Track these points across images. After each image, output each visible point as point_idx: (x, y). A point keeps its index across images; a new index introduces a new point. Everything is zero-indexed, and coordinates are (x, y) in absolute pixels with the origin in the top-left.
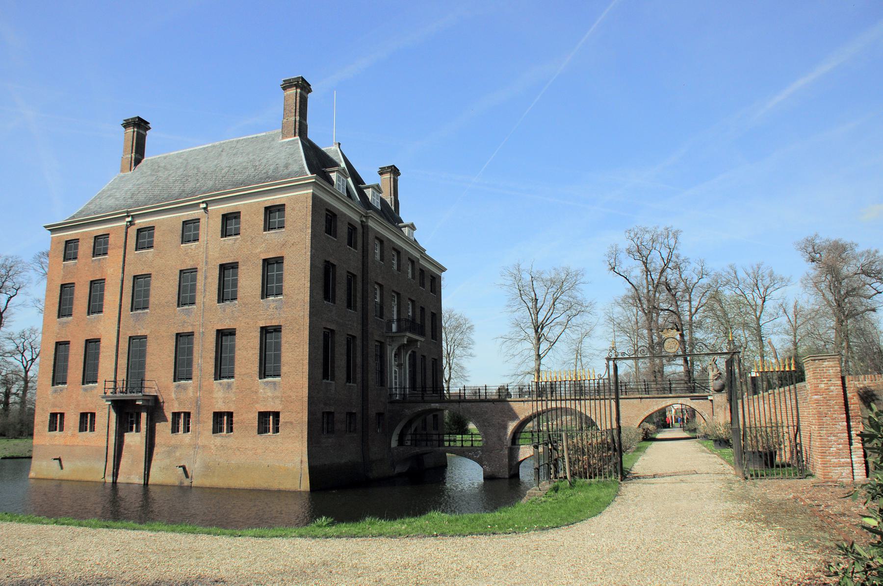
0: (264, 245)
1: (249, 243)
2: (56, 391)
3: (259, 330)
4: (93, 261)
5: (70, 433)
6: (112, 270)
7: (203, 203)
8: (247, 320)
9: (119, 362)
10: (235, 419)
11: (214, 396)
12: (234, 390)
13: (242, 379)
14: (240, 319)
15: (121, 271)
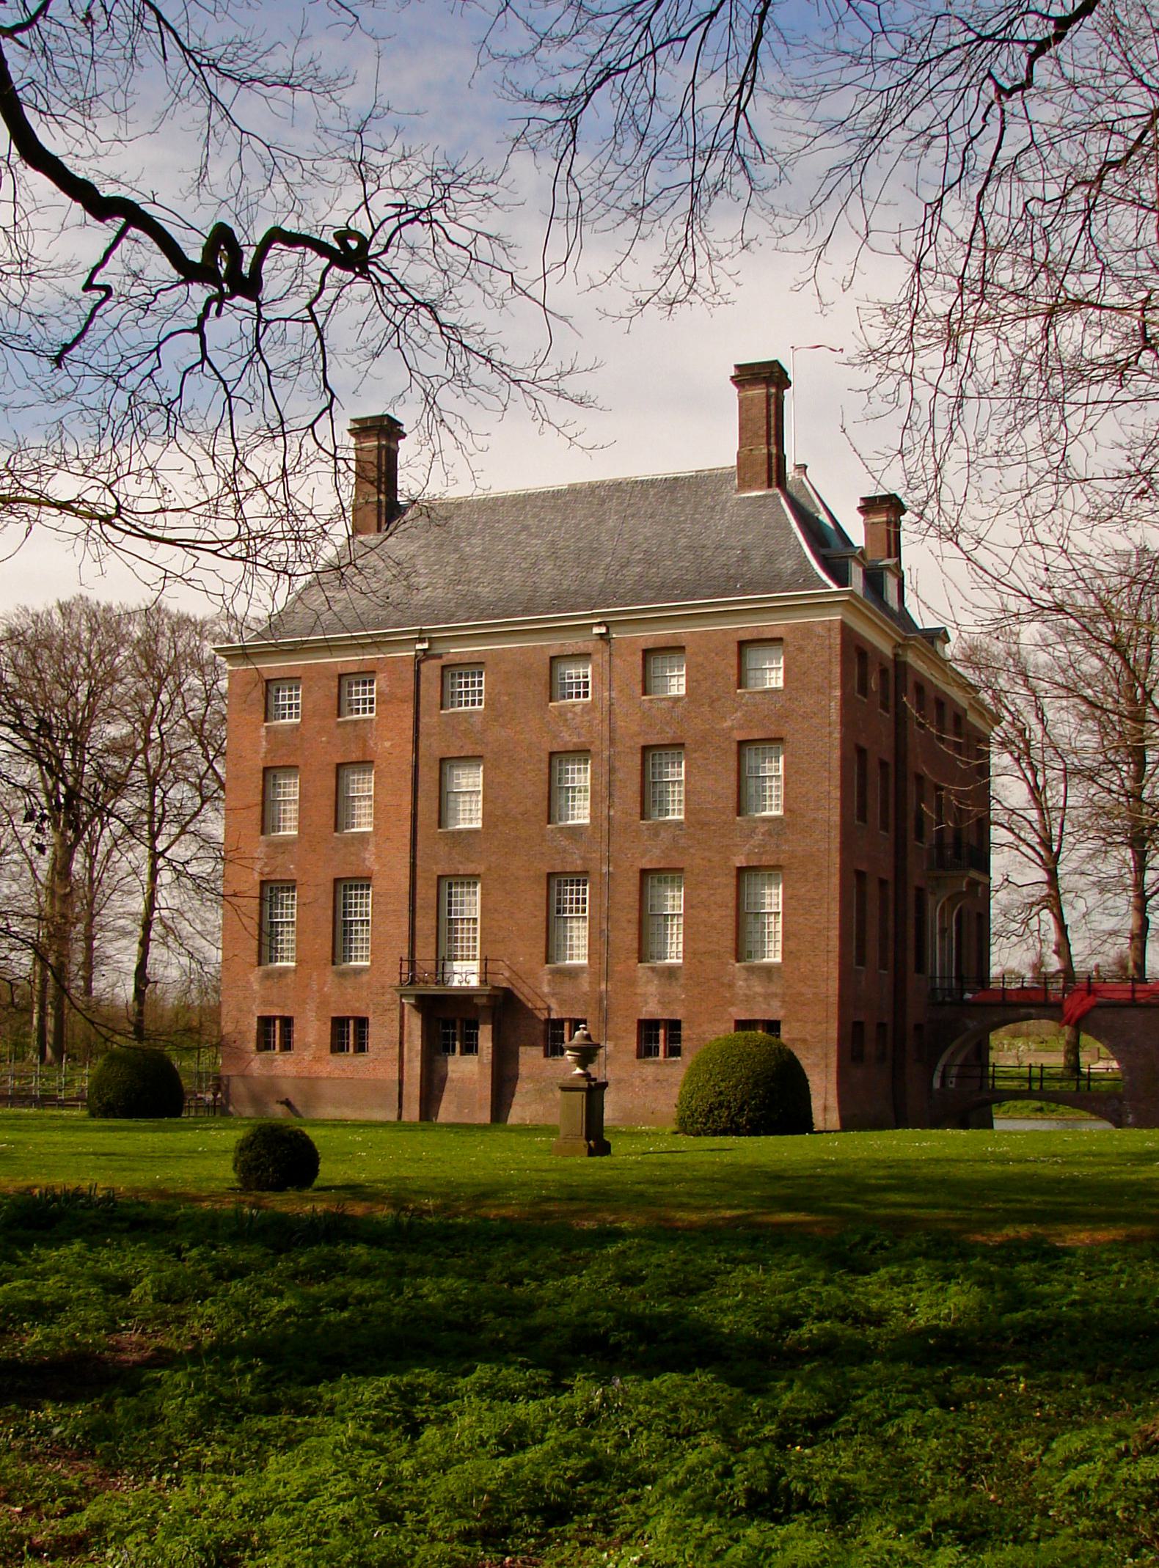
0: (739, 714)
1: (706, 708)
2: (268, 976)
3: (734, 873)
4: (339, 724)
5: (308, 1056)
6: (387, 744)
7: (599, 624)
8: (707, 854)
9: (418, 924)
10: (685, 1033)
11: (639, 991)
12: (682, 981)
13: (700, 962)
14: (692, 851)
15: (410, 747)
